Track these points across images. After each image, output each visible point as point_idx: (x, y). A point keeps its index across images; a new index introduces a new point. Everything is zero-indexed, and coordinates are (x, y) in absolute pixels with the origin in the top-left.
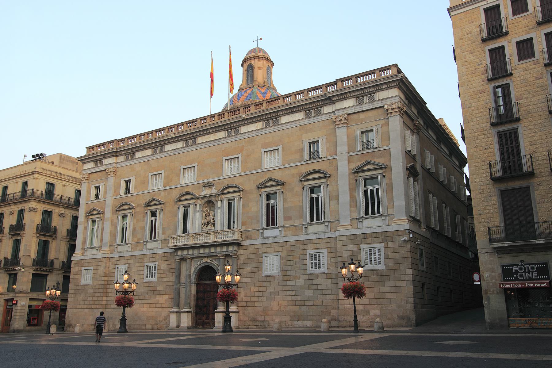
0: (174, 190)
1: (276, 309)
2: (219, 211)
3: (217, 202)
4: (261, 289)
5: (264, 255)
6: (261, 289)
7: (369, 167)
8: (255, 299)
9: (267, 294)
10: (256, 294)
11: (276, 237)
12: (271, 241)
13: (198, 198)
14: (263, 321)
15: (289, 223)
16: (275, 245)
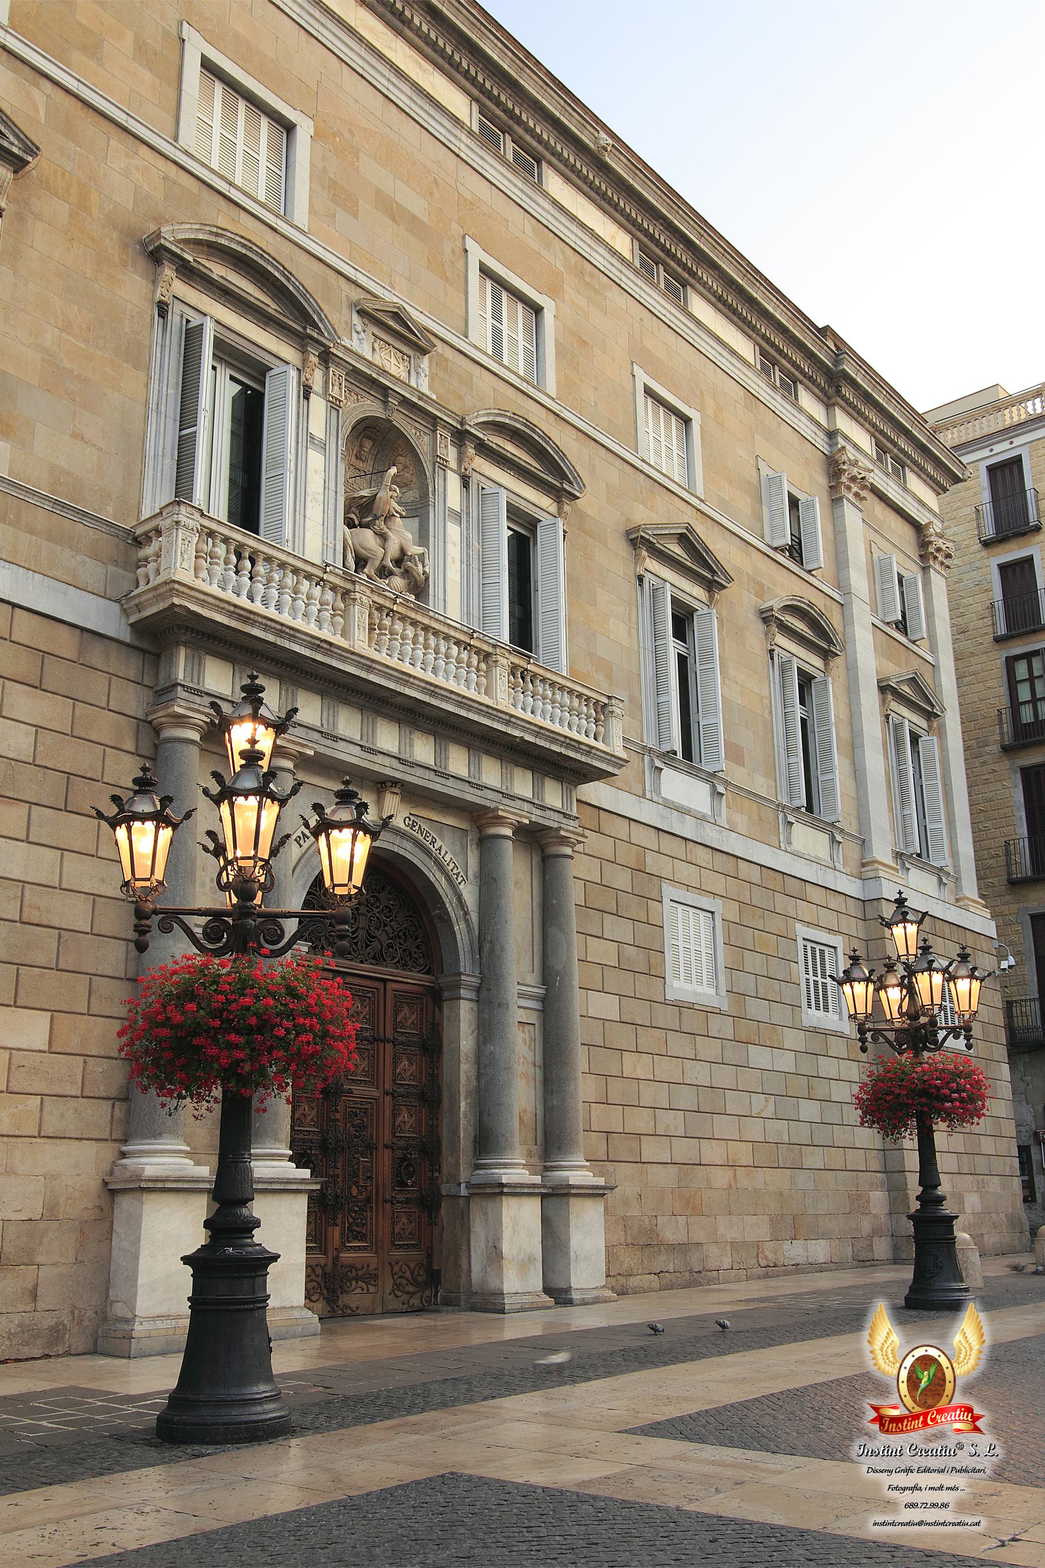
0: (117, 143)
1: (721, 1178)
2: (454, 531)
3: (444, 466)
4: (667, 1069)
5: (669, 891)
6: (667, 1069)
7: (906, 689)
8: (640, 1121)
9: (686, 1099)
10: (649, 1094)
11: (702, 818)
12: (687, 828)
13: (326, 358)
14: (682, 1248)
15: (738, 775)
16: (702, 856)
